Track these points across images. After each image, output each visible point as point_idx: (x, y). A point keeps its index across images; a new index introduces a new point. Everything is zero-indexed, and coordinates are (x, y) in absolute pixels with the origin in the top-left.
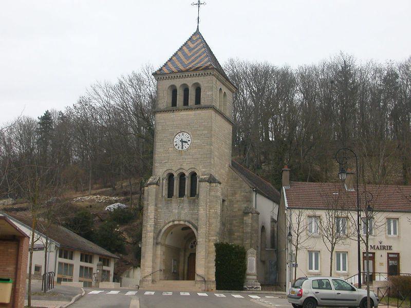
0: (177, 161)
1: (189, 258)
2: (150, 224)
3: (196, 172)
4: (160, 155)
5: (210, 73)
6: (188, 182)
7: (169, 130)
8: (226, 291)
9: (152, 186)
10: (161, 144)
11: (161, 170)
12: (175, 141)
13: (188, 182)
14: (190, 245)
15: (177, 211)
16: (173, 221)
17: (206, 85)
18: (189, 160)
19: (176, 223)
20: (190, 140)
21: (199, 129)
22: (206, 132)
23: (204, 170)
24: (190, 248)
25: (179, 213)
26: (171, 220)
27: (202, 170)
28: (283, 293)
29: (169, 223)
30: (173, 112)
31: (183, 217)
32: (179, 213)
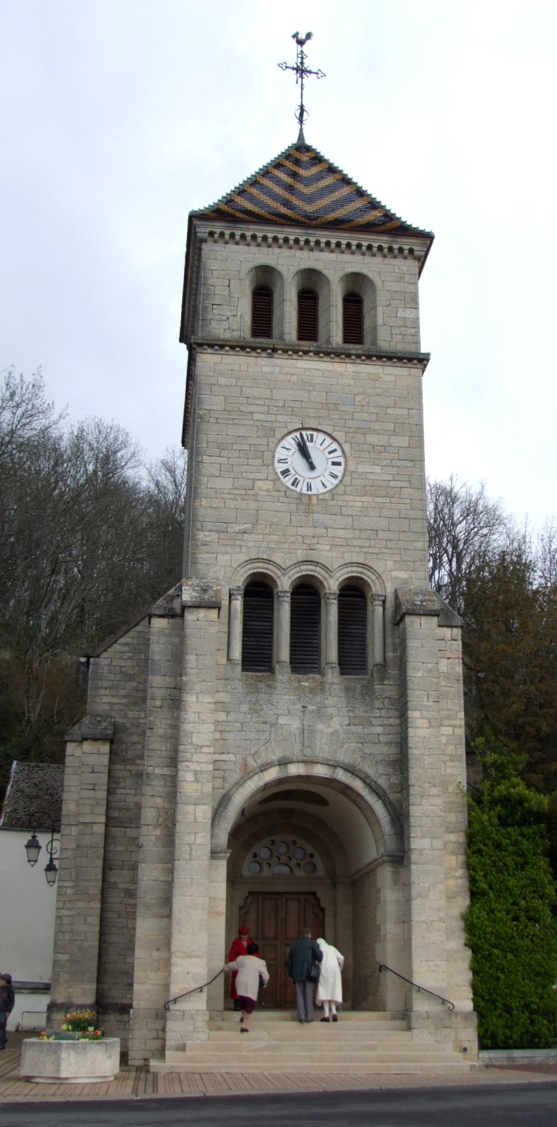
0: (291, 531)
2: (194, 766)
3: (369, 577)
4: (216, 503)
5: (411, 251)
6: (331, 615)
9: (202, 614)
10: (224, 460)
11: (224, 559)
12: (278, 456)
13: (331, 615)
15: (296, 724)
16: (284, 763)
17: (395, 286)
18: (341, 533)
19: (295, 770)
20: (341, 460)
21: (377, 426)
22: (398, 441)
23: (403, 575)
26: (275, 758)
27: (394, 574)
29: (263, 768)
30: (270, 356)
31: (323, 748)
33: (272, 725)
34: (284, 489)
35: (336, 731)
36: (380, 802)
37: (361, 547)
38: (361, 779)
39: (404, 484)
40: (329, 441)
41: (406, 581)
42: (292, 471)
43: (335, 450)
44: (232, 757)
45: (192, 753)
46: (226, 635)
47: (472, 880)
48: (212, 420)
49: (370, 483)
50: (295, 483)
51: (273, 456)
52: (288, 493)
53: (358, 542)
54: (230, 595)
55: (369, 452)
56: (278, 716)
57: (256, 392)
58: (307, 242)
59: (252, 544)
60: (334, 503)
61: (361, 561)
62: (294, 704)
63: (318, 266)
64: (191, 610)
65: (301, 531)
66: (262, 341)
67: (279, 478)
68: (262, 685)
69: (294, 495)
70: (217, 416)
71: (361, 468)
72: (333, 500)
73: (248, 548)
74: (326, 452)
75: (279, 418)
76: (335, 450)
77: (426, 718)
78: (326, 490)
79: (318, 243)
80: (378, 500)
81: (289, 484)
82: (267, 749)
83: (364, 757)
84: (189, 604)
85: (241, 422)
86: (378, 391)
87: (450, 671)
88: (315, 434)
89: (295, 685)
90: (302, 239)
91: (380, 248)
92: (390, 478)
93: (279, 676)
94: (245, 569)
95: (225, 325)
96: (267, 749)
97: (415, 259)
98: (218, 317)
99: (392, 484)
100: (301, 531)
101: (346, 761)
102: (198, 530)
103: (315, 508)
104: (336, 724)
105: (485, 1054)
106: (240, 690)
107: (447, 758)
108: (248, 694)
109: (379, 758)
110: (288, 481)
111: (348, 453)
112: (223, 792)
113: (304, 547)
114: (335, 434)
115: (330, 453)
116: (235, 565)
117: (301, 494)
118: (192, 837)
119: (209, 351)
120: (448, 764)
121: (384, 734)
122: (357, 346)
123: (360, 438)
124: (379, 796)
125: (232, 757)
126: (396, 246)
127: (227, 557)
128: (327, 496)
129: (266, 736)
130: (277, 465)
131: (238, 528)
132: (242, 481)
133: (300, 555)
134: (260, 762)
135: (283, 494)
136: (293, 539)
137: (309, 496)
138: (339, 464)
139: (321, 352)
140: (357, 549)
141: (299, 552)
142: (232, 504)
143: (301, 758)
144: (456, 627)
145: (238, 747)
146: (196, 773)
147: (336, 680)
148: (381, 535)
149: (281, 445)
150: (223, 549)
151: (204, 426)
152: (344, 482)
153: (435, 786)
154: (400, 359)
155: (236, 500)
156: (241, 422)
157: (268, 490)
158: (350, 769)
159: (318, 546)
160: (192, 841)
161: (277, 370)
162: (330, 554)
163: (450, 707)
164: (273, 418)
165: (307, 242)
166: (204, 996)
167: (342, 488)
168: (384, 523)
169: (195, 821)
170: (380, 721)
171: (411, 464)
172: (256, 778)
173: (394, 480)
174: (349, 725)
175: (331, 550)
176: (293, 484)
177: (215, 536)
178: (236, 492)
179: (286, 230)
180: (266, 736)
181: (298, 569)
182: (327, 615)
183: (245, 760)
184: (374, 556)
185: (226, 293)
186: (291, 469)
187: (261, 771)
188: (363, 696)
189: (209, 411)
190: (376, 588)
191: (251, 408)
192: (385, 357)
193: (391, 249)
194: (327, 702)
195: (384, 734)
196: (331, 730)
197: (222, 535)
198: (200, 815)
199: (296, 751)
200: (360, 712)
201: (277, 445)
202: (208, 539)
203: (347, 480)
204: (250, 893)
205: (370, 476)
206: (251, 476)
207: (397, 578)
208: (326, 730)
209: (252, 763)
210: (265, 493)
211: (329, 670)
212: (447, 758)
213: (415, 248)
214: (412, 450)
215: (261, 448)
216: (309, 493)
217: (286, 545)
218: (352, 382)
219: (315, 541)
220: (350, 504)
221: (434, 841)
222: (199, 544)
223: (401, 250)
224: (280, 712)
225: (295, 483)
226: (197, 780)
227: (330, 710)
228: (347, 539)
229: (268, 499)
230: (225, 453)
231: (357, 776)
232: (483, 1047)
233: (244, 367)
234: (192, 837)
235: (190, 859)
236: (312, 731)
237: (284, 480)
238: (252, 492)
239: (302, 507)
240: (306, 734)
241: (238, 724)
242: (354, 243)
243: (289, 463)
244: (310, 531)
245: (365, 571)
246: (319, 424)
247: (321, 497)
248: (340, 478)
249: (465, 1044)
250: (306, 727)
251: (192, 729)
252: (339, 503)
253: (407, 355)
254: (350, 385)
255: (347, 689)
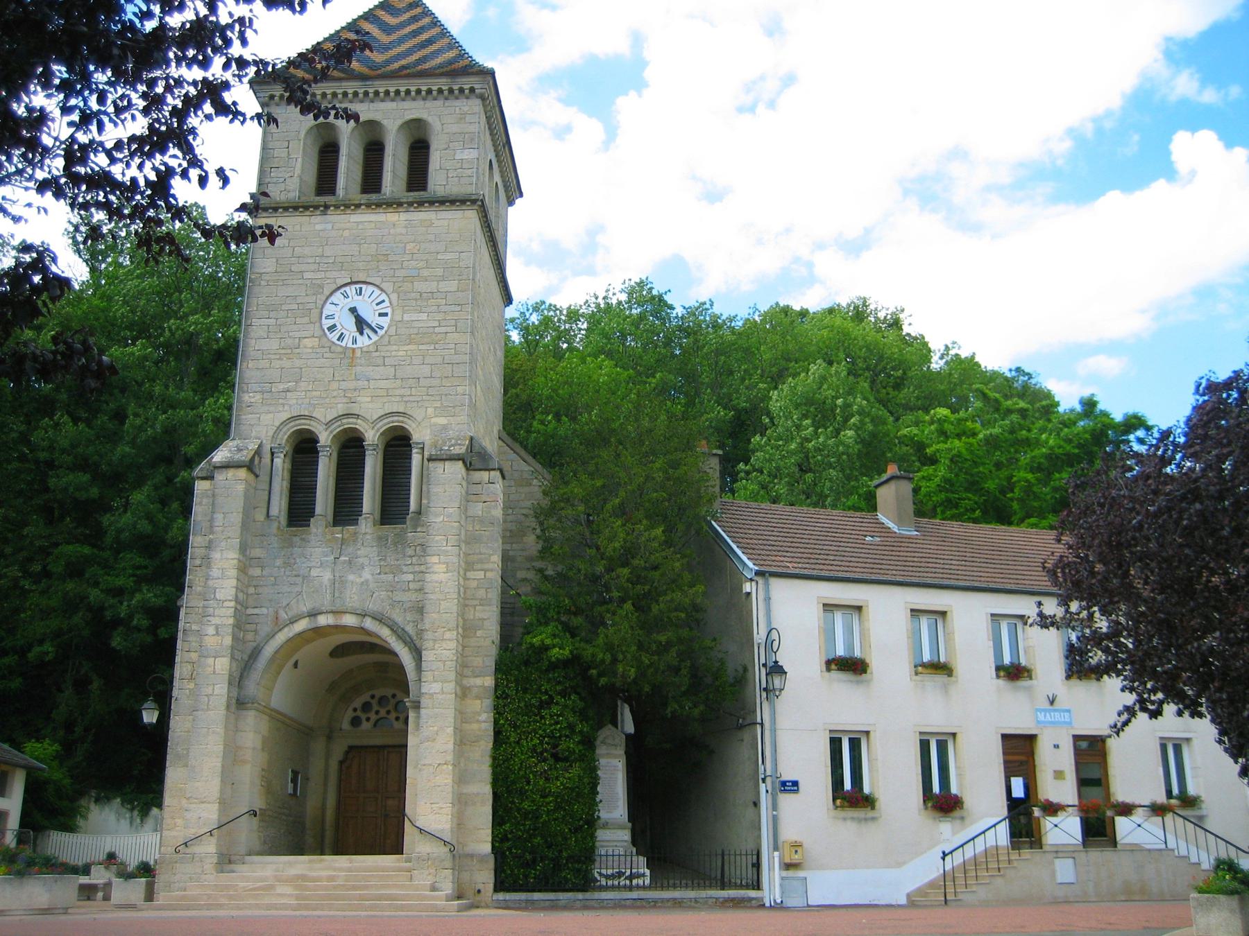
0: (335, 385)
1: (341, 763)
3: (411, 426)
5: (472, 90)
6: (372, 467)
7: (307, 275)
8: (537, 896)
9: (231, 473)
10: (272, 321)
11: (267, 418)
12: (325, 312)
13: (372, 467)
14: (350, 714)
15: (327, 576)
16: (313, 615)
17: (455, 128)
18: (383, 384)
19: (323, 620)
20: (389, 311)
21: (425, 273)
22: (452, 285)
23: (442, 421)
24: (346, 725)
25: (338, 584)
28: (752, 893)
29: (293, 622)
30: (324, 213)
31: (352, 598)
32: (338, 584)
33: (304, 577)
34: (328, 344)
35: (367, 581)
36: (407, 648)
37: (402, 396)
38: (388, 627)
39: (449, 329)
40: (377, 292)
41: (445, 428)
42: (339, 327)
43: (383, 301)
44: (264, 611)
45: (214, 608)
46: (267, 493)
47: (496, 722)
48: (263, 283)
49: (415, 331)
50: (341, 338)
51: (322, 313)
52: (333, 348)
53: (398, 392)
54: (272, 454)
55: (416, 300)
56: (310, 568)
57: (307, 251)
58: (366, 94)
59: (295, 401)
60: (378, 354)
61: (401, 410)
62: (326, 556)
63: (423, 115)
64: (220, 470)
65: (344, 385)
66: (322, 200)
67: (325, 334)
68: (296, 539)
69: (339, 349)
70: (267, 278)
71: (406, 317)
72: (377, 351)
73: (291, 406)
74: (374, 304)
75: (328, 275)
76: (383, 301)
77: (444, 563)
78: (371, 342)
79: (377, 93)
80: (421, 347)
81: (335, 340)
82: (298, 600)
83: (393, 605)
84: (218, 465)
85: (290, 282)
86: (432, 237)
87: (485, 514)
88: (364, 287)
89: (329, 537)
90: (361, 91)
91: (440, 91)
92: (436, 324)
93: (313, 528)
94: (288, 427)
95: (282, 187)
96: (298, 600)
97: (477, 97)
98: (275, 180)
99: (437, 330)
100: (344, 385)
101: (375, 609)
102: (243, 392)
103: (358, 361)
104: (366, 575)
105: (501, 896)
106: (276, 545)
107: (477, 602)
108: (283, 548)
109: (408, 605)
110: (333, 337)
111: (395, 303)
112: (254, 644)
113: (345, 400)
114: (384, 286)
115: (377, 304)
116: (277, 424)
117: (346, 348)
118: (211, 688)
119: (265, 214)
120: (477, 608)
121: (414, 581)
122: (422, 193)
123: (407, 286)
124: (405, 643)
125: (264, 611)
126: (456, 87)
127: (271, 416)
128: (371, 349)
129: (298, 589)
130: (324, 321)
131: (281, 387)
132: (289, 341)
133: (341, 409)
134: (291, 614)
135: (327, 350)
136: (335, 394)
137: (354, 350)
138: (386, 315)
139: (373, 204)
140: (398, 399)
141: (340, 406)
142: (277, 364)
143: (329, 608)
144: (494, 470)
145: (270, 601)
146: (217, 628)
147: (368, 530)
148: (423, 382)
149: (330, 301)
150: (266, 408)
151: (256, 289)
152: (388, 333)
153: (449, 630)
154: (453, 202)
155: (282, 359)
156: (290, 282)
157: (313, 348)
158: (379, 618)
159: (359, 399)
160: (210, 692)
161: (329, 226)
162: (370, 405)
163: (483, 551)
164: (322, 275)
165: (366, 94)
166: (213, 840)
167: (386, 339)
168: (426, 370)
169: (214, 672)
170: (411, 569)
171: (459, 308)
172: (286, 629)
173: (440, 326)
174: (380, 574)
175: (372, 402)
176: (338, 340)
177: (258, 396)
178: (283, 351)
179: (344, 84)
180: (298, 589)
181: (339, 423)
182: (374, 467)
183: (277, 612)
184: (415, 404)
185: (284, 155)
186: (338, 325)
187: (292, 623)
188: (395, 544)
189: (261, 274)
190: (416, 437)
191: (303, 268)
192: (437, 202)
193: (451, 91)
194: (359, 552)
195: (414, 581)
196: (362, 580)
197: (266, 396)
198: (218, 667)
199: (326, 601)
200: (391, 560)
201: (325, 302)
202: (252, 400)
204: (351, 748)
205: (416, 324)
206: (297, 335)
207: (435, 425)
208: (358, 580)
209: (283, 615)
210: (310, 351)
211: (363, 521)
212: (477, 602)
213: (476, 86)
214: (460, 294)
215: (309, 306)
216: (355, 346)
217: (327, 400)
218: (404, 231)
219: (356, 394)
220: (393, 353)
221: (445, 685)
222: (244, 405)
223: (461, 90)
224: (314, 564)
225: (341, 338)
226: (217, 634)
227: (361, 560)
228: (387, 389)
229: (313, 355)
230: (272, 314)
231: (384, 624)
232: (497, 888)
233: (298, 227)
234: (211, 688)
235: (208, 709)
236: (343, 582)
237: (330, 336)
238: (298, 351)
239: (346, 361)
240: (337, 585)
241: (272, 579)
242: (392, 90)
243: (337, 318)
244: (352, 385)
245: (405, 420)
246: (368, 276)
247: (365, 349)
248: (385, 329)
249: (480, 886)
250: (337, 578)
251: (216, 585)
252: (383, 354)
253: (459, 198)
254: (401, 234)
255: (380, 538)
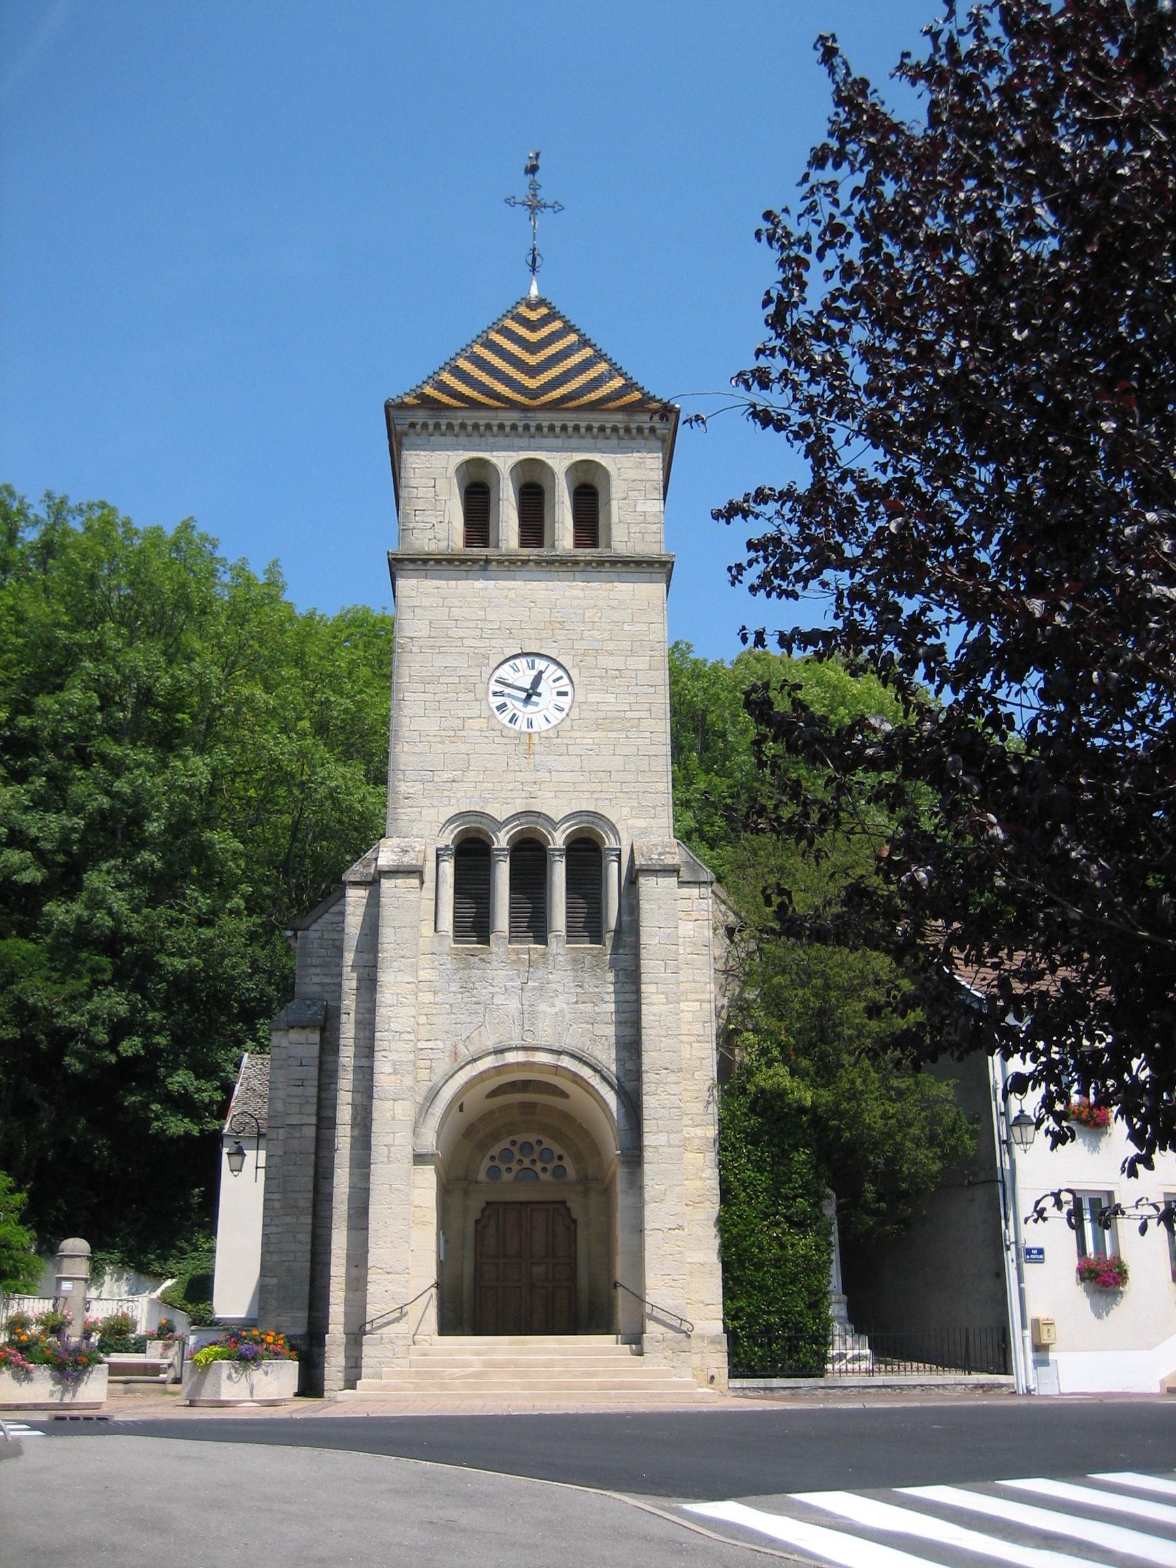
1: (477, 1222)
2: (393, 1056)
4: (419, 748)
7: (467, 642)
8: (776, 1382)
11: (429, 814)
14: (486, 1163)
15: (513, 1005)
18: (568, 777)
20: (569, 689)
21: (611, 646)
24: (482, 1176)
25: (527, 1016)
26: (490, 1043)
27: (631, 822)
28: (1002, 1379)
32: (527, 1016)
34: (499, 727)
41: (644, 832)
43: (561, 678)
47: (723, 1181)
49: (603, 715)
51: (488, 689)
52: (505, 731)
53: (587, 787)
54: (438, 856)
58: (527, 427)
60: (559, 740)
65: (520, 777)
66: (477, 552)
67: (493, 715)
69: (512, 734)
71: (592, 697)
75: (494, 643)
76: (561, 678)
78: (550, 726)
80: (610, 735)
84: (386, 869)
85: (448, 650)
86: (614, 603)
90: (521, 424)
95: (430, 534)
97: (658, 439)
98: (421, 525)
99: (629, 715)
100: (520, 777)
104: (561, 1003)
105: (738, 1383)
107: (693, 1039)
113: (524, 794)
115: (555, 681)
119: (411, 567)
126: (633, 426)
127: (433, 810)
128: (552, 734)
131: (446, 776)
137: (530, 734)
138: (565, 694)
142: (439, 748)
143: (519, 1043)
146: (394, 1063)
148: (615, 777)
151: (406, 657)
167: (568, 722)
168: (618, 762)
171: (652, 690)
174: (576, 1003)
176: (510, 721)
178: (444, 733)
180: (479, 1019)
185: (430, 493)
190: (610, 842)
193: (627, 430)
196: (556, 1010)
197: (428, 786)
198: (399, 1113)
202: (411, 791)
203: (575, 714)
204: (488, 1203)
211: (554, 940)
215: (472, 680)
216: (530, 730)
219: (536, 787)
224: (496, 989)
230: (429, 688)
232: (733, 1375)
236: (534, 1014)
239: (522, 748)
244: (531, 777)
245: (596, 820)
246: (541, 647)
247: (543, 734)
248: (566, 711)
249: (713, 1372)
252: (565, 741)
